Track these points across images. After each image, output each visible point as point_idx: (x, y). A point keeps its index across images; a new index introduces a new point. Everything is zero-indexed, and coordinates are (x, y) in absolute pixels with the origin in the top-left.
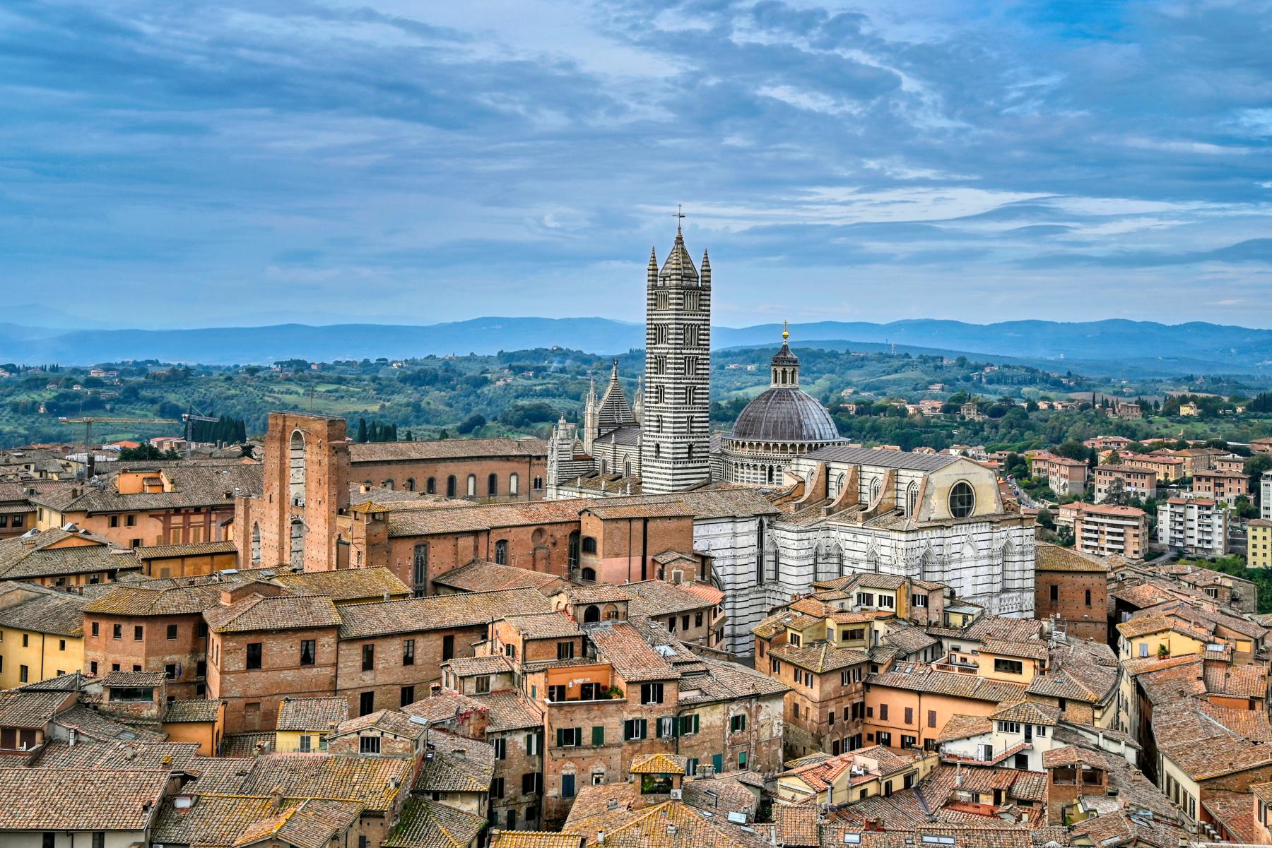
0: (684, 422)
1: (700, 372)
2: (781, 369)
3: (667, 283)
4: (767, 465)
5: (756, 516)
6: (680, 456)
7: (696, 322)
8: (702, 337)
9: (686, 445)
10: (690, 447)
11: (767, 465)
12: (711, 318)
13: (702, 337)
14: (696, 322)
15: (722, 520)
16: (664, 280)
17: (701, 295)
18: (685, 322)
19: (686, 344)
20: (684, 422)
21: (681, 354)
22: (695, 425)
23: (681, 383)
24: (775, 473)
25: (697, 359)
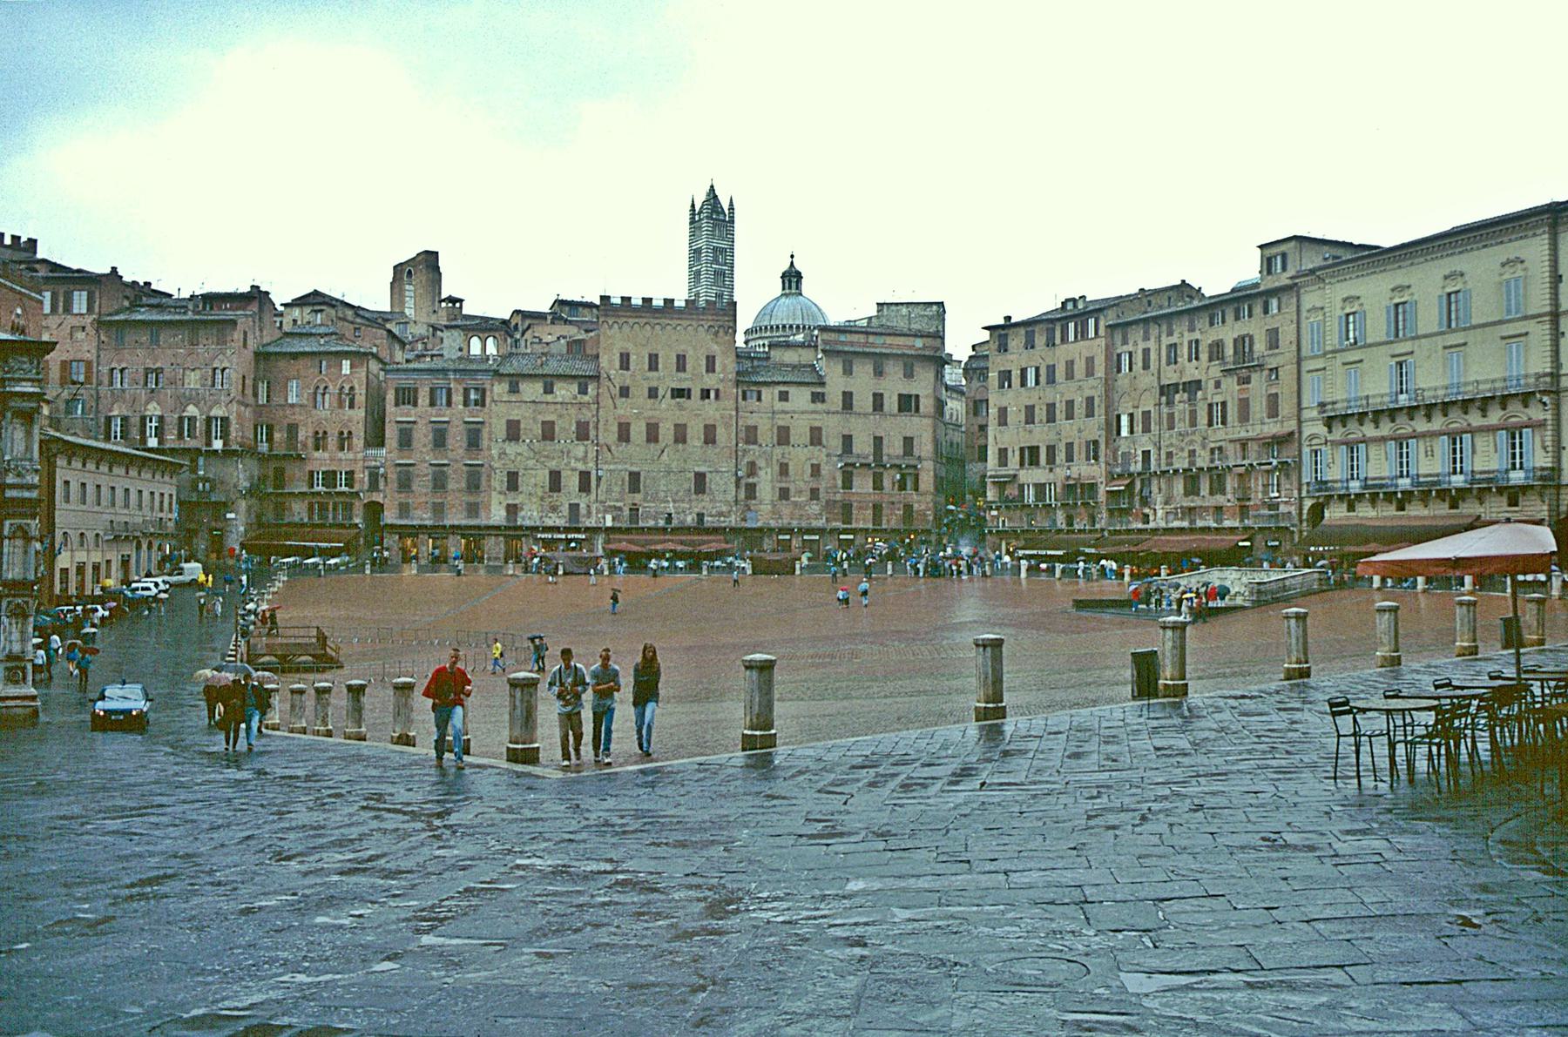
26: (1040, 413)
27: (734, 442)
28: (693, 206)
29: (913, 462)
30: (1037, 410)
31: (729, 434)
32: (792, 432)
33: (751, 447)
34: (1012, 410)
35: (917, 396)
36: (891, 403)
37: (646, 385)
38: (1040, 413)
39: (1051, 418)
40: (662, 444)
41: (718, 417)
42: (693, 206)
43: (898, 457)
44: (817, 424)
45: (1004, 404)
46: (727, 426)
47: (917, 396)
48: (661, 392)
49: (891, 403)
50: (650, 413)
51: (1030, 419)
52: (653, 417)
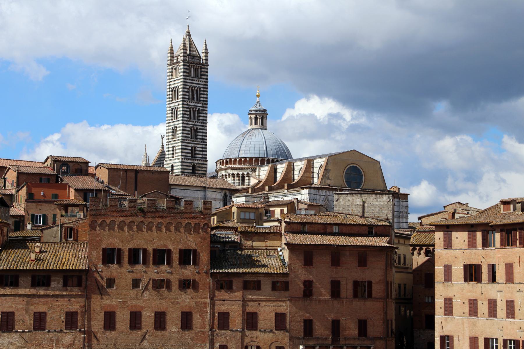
0: (189, 150)
1: (201, 118)
2: (254, 116)
3: (179, 60)
4: (241, 173)
5: (222, 189)
6: (186, 171)
7: (198, 86)
8: (202, 96)
9: (190, 164)
10: (194, 167)
11: (241, 173)
12: (209, 84)
13: (202, 96)
14: (198, 86)
15: (197, 189)
16: (177, 59)
17: (201, 68)
18: (190, 84)
19: (191, 99)
20: (189, 150)
21: (187, 105)
22: (197, 152)
23: (187, 124)
24: (246, 178)
25: (199, 110)
26: (483, 308)
27: (208, 328)
28: (172, 50)
29: (367, 343)
30: (479, 303)
31: (203, 319)
32: (260, 318)
33: (223, 332)
34: (456, 303)
35: (370, 283)
36: (347, 289)
37: (130, 277)
38: (483, 308)
39: (493, 313)
40: (144, 330)
41: (193, 305)
42: (172, 50)
43: (354, 339)
44: (281, 310)
45: (450, 294)
46: (202, 313)
47: (370, 283)
48: (144, 282)
49: (347, 289)
50: (134, 302)
51: (473, 310)
52: (135, 306)
